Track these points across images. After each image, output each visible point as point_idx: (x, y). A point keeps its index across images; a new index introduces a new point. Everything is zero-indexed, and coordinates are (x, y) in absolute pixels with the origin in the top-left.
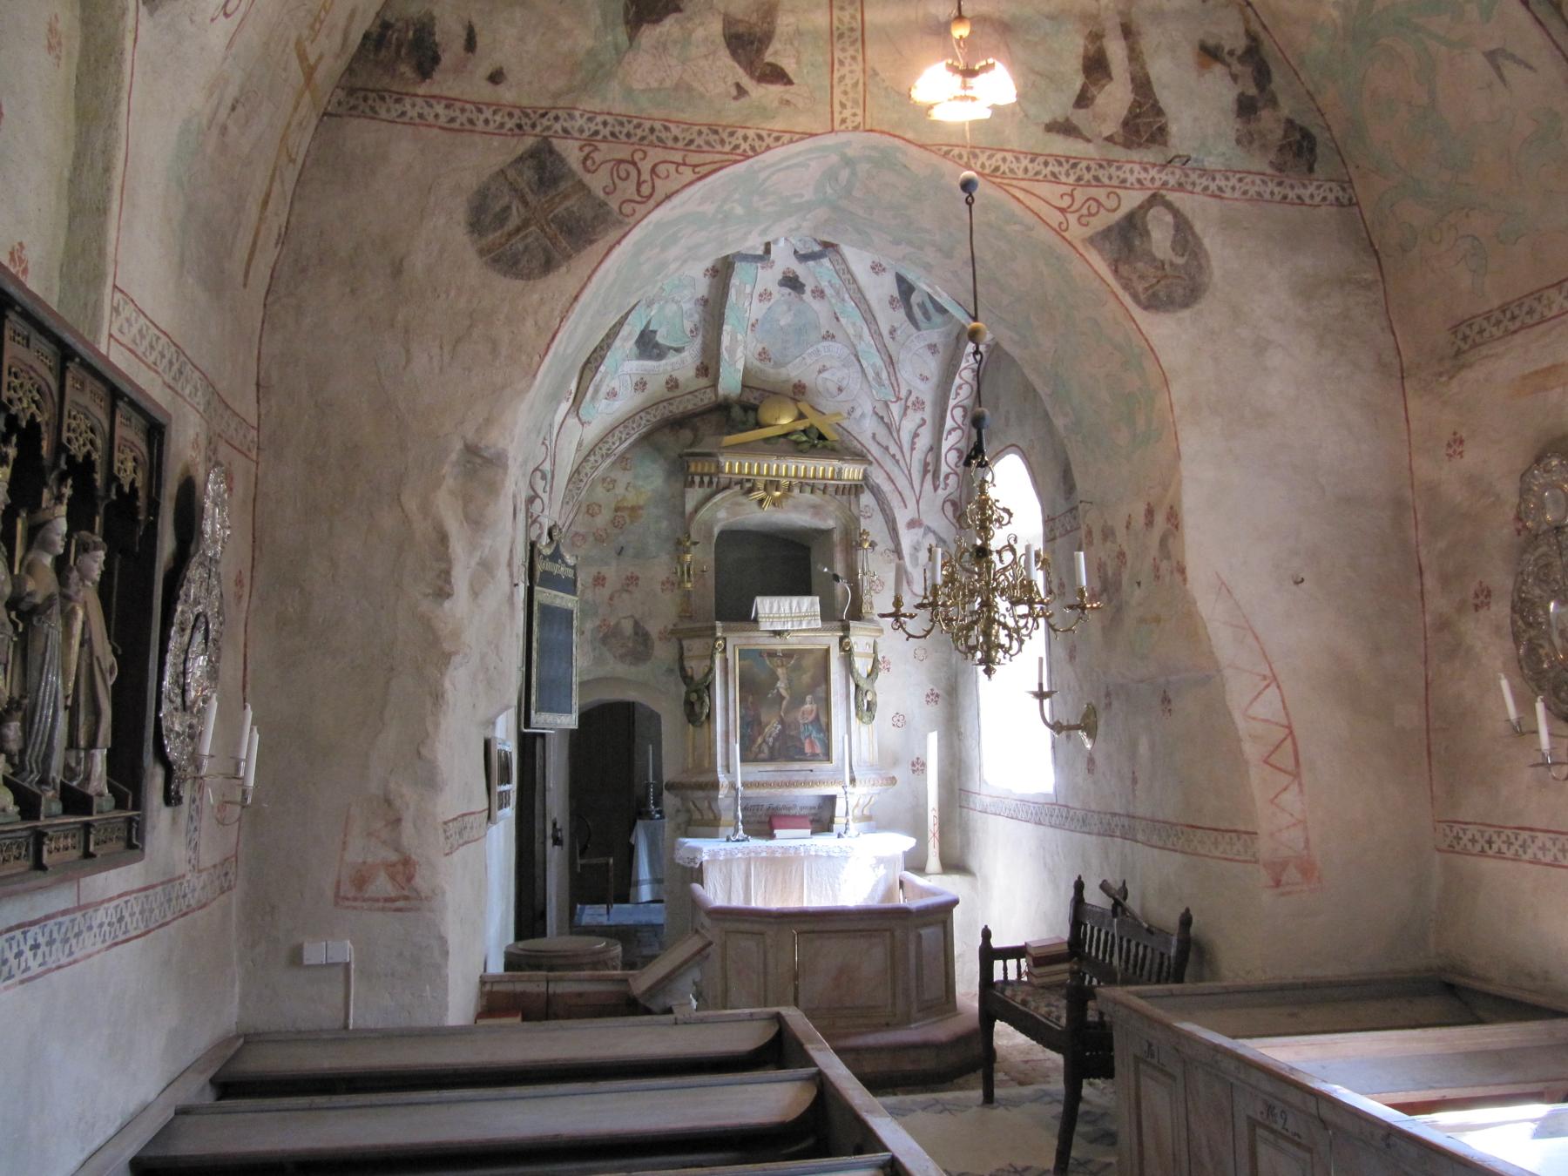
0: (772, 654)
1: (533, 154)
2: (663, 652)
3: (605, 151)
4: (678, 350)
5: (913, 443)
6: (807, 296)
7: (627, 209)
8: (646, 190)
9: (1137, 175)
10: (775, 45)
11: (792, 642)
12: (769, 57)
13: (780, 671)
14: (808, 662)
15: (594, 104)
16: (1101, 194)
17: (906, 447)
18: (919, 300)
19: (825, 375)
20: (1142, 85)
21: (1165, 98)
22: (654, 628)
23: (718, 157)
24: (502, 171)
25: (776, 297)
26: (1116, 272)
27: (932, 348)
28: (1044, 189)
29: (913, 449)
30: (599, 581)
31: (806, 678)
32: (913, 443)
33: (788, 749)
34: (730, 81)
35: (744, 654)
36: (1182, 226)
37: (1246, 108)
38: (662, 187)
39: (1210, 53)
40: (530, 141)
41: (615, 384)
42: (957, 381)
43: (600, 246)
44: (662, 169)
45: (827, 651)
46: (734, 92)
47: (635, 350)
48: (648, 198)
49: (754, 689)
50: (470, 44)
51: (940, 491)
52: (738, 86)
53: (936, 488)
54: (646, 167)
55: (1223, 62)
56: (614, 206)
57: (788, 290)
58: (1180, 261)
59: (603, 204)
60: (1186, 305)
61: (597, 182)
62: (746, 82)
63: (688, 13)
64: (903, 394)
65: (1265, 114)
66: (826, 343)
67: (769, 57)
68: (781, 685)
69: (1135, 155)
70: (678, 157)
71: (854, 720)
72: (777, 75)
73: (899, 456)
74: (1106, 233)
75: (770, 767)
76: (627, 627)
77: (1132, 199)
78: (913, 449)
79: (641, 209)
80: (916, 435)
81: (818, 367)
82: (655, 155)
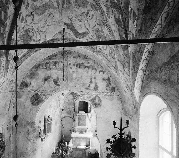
0: (81, 116)
1: (36, 94)
2: (72, 114)
3: (42, 94)
7: (44, 99)
8: (46, 97)
9: (95, 94)
10: (59, 82)
11: (83, 115)
12: (58, 83)
13: (82, 118)
14: (84, 117)
15: (41, 89)
16: (91, 95)
20: (96, 84)
21: (98, 85)
22: (71, 112)
23: (53, 94)
24: (33, 96)
26: (92, 104)
28: (86, 95)
30: (67, 107)
31: (84, 118)
33: (83, 125)
34: (54, 86)
35: (78, 116)
36: (99, 99)
37: (108, 85)
38: (48, 97)
39: (104, 79)
40: (36, 93)
43: (42, 103)
44: (48, 95)
45: (86, 116)
46: (54, 87)
48: (46, 98)
49: (79, 119)
50: (30, 84)
52: (55, 86)
54: (46, 95)
55: (105, 81)
56: (43, 99)
58: (99, 102)
59: (42, 99)
60: (99, 107)
61: (42, 97)
62: (56, 86)
63: (50, 79)
65: (110, 86)
67: (58, 83)
68: (82, 119)
69: (95, 91)
70: (49, 94)
71: (89, 122)
72: (59, 85)
74: (91, 100)
75: (81, 126)
76: (69, 112)
77: (94, 96)
79: (46, 99)
82: (47, 94)
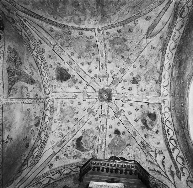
4: (88, 151)
5: (164, 165)
6: (121, 135)
17: (162, 168)
18: (148, 122)
19: (129, 155)
25: (113, 137)
27: (157, 132)
29: (164, 167)
32: (164, 165)
41: (68, 153)
42: (167, 128)
47: (76, 146)
51: (183, 178)
53: (180, 178)
57: (116, 135)
64: (154, 150)
66: (128, 147)
73: (160, 170)
78: (164, 167)
80: (163, 162)
81: (127, 153)
